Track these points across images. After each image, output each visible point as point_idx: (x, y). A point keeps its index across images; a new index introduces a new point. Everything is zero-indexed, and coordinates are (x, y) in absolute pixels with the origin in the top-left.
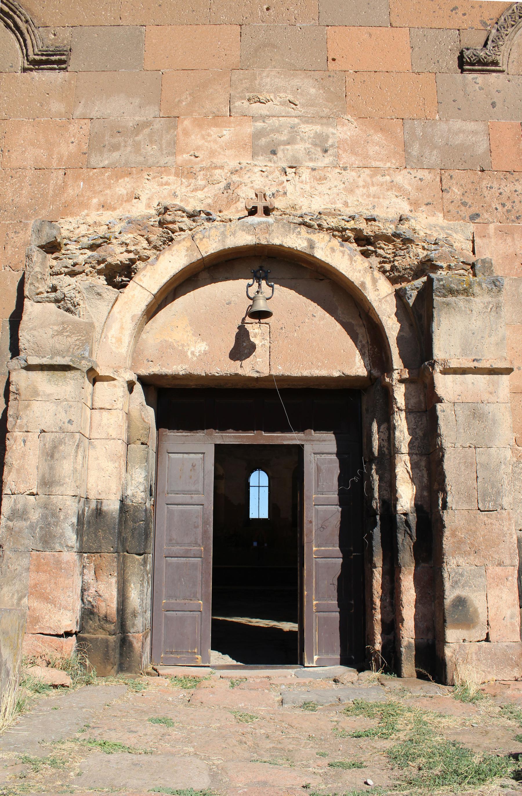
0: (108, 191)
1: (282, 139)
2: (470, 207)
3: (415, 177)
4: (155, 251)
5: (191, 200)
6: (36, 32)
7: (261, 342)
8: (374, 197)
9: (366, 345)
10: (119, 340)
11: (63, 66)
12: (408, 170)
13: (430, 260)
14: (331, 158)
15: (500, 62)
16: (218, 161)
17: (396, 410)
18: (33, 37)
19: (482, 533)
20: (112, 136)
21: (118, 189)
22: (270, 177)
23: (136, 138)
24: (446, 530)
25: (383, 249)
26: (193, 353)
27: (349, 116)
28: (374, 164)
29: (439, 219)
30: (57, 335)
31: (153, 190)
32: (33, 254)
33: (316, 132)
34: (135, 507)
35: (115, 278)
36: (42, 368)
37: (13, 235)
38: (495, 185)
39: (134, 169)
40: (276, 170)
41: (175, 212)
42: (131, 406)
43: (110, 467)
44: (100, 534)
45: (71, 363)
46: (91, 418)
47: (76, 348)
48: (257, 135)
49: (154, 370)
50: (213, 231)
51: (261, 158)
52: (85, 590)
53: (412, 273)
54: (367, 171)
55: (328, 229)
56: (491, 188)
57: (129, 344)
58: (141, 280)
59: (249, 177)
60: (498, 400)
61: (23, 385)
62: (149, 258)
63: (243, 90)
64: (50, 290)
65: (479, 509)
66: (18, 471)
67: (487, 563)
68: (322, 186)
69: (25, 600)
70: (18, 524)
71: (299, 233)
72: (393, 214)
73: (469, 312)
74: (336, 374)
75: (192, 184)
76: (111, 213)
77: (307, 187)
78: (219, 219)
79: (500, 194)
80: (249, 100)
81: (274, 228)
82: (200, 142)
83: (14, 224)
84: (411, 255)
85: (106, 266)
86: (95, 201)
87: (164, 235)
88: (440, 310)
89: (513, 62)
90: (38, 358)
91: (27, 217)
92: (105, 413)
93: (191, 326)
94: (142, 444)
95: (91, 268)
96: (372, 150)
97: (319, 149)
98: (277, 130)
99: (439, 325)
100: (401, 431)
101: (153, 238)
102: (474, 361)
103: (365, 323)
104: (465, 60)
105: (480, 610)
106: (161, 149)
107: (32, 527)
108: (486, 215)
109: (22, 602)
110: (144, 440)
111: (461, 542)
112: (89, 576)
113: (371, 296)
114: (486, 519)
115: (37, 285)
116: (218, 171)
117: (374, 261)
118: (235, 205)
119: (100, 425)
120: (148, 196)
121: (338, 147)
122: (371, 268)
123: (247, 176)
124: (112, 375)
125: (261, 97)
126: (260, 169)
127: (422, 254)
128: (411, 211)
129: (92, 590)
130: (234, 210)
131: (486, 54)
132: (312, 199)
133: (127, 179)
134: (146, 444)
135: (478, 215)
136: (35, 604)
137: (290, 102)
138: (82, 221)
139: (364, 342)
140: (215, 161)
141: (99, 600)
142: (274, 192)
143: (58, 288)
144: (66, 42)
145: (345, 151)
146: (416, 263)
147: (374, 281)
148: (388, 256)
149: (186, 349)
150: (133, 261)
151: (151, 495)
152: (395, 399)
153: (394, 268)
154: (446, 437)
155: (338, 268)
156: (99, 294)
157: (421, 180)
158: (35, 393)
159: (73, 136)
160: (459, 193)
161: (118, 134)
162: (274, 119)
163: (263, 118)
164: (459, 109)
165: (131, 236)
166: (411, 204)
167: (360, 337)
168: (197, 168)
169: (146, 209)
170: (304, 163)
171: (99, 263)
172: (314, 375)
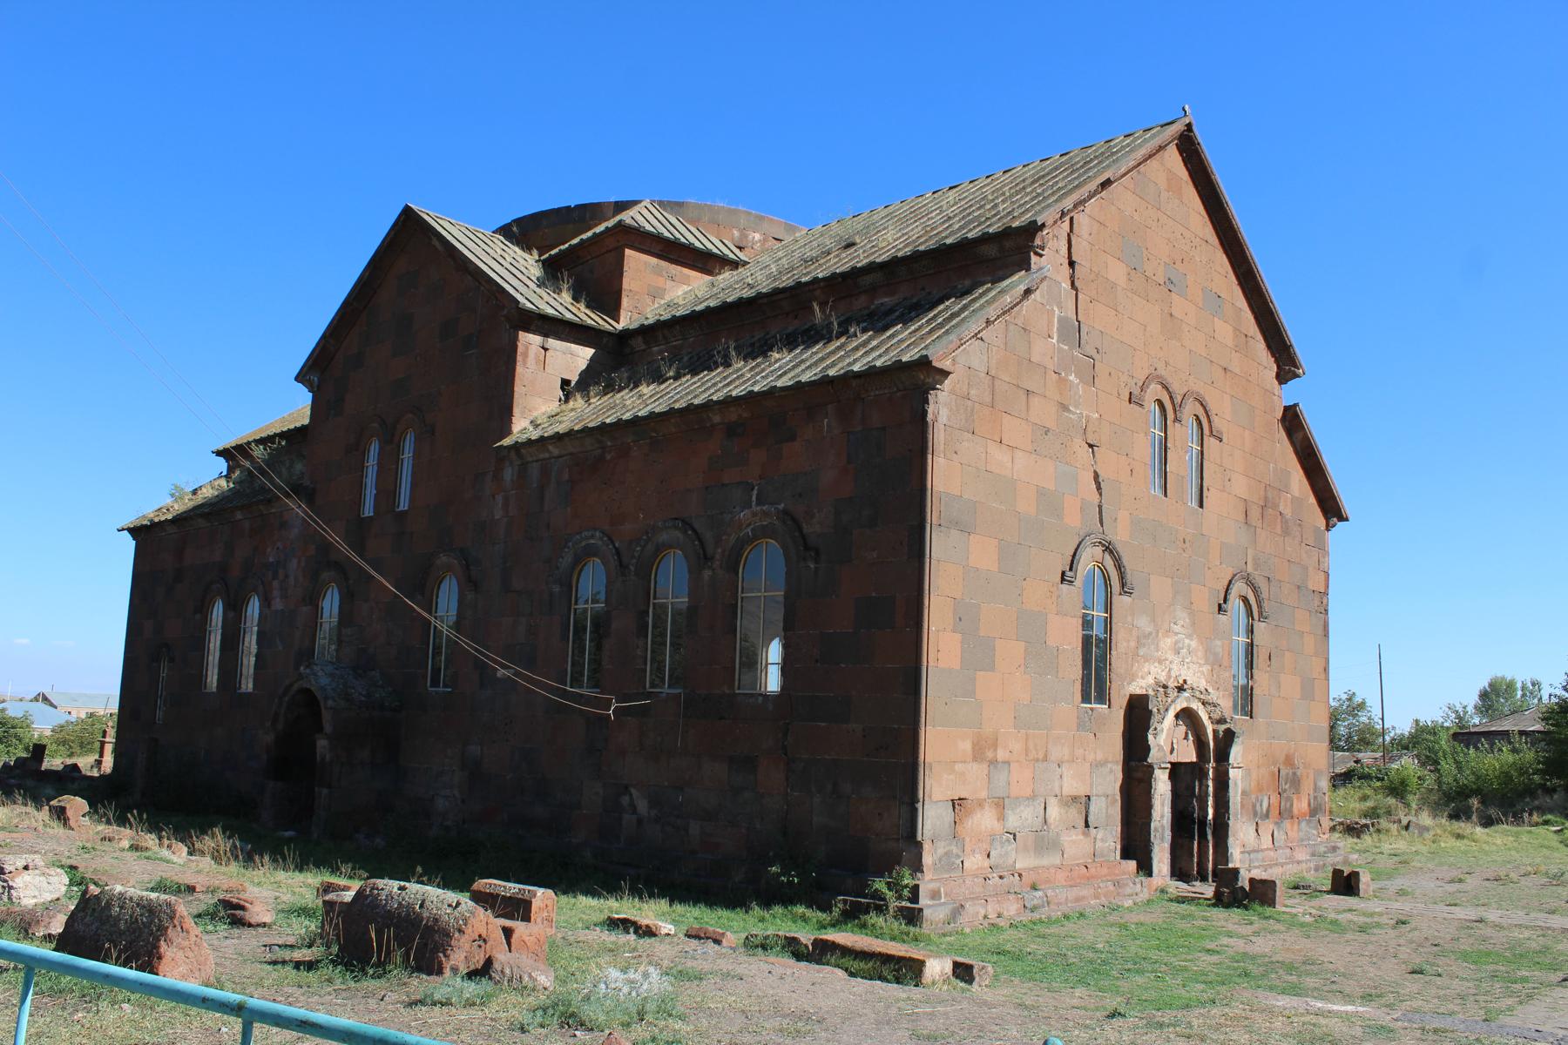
28: (1200, 661)
48: (1176, 643)
163: (1177, 634)
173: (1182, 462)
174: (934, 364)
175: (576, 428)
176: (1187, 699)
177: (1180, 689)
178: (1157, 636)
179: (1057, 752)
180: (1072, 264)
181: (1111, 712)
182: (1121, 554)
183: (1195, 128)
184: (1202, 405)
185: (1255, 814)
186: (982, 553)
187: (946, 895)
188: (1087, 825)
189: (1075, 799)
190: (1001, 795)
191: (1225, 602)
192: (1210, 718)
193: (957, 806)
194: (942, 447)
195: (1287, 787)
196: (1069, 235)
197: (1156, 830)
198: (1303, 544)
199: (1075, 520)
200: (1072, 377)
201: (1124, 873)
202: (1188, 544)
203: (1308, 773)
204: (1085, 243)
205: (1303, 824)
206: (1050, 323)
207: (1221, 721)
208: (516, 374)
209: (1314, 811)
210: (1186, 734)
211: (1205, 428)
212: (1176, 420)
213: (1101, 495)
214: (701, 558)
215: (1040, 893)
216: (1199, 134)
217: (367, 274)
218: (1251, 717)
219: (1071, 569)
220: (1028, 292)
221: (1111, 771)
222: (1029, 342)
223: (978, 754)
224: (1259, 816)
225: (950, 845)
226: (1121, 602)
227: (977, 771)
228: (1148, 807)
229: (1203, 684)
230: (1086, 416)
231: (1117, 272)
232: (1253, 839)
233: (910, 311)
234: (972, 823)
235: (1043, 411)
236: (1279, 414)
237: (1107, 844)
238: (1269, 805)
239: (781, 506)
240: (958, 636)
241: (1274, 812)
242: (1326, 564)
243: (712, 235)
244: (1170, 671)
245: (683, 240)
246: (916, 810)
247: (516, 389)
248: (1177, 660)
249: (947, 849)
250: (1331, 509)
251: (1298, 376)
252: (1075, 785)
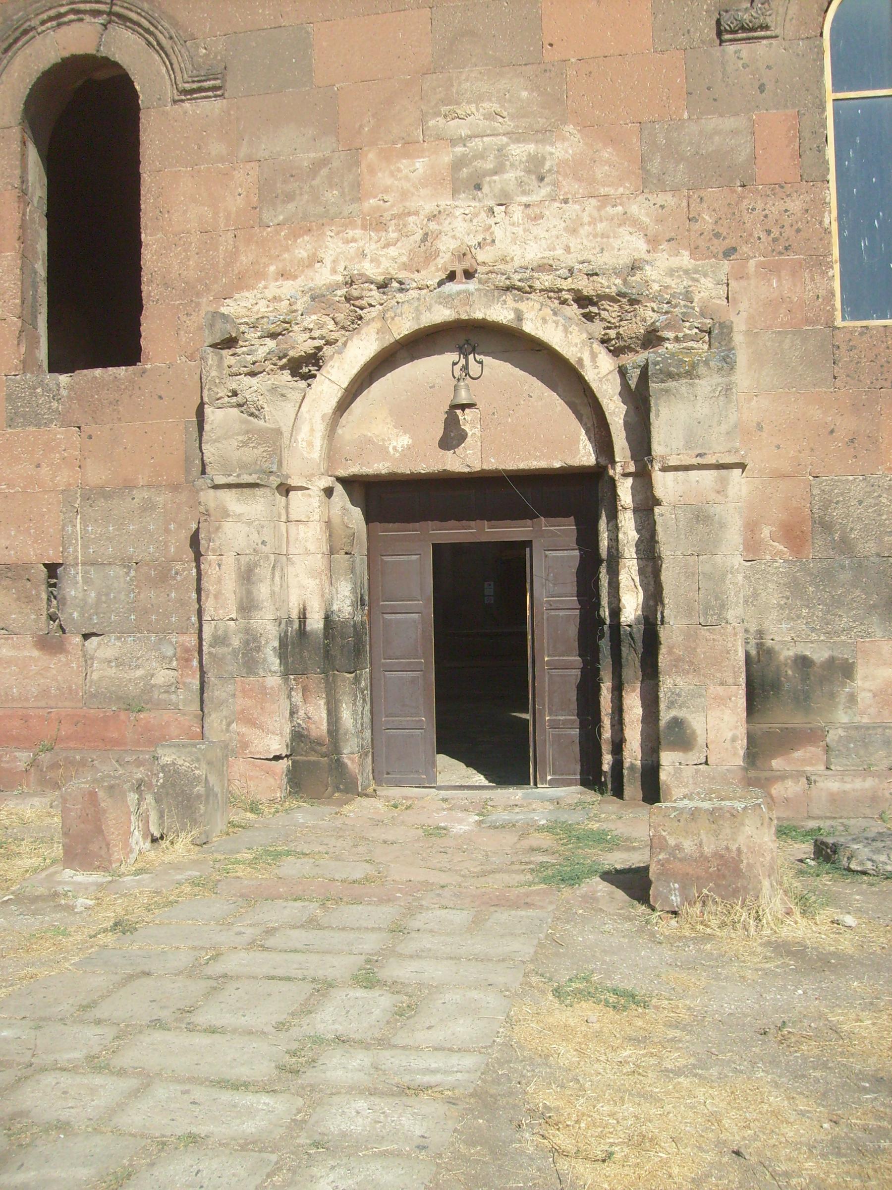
0: (286, 256)
1: (488, 168)
2: (724, 238)
3: (654, 204)
4: (343, 332)
5: (383, 259)
6: (183, 51)
7: (471, 430)
8: (603, 236)
9: (592, 428)
10: (310, 444)
11: (219, 93)
12: (646, 196)
13: (655, 331)
14: (549, 189)
15: (772, 25)
16: (412, 205)
17: (620, 508)
18: (180, 58)
19: (703, 650)
20: (284, 182)
21: (297, 251)
22: (475, 221)
23: (313, 183)
24: (662, 646)
25: (608, 311)
26: (395, 448)
27: (572, 126)
28: (603, 191)
29: (685, 260)
30: (242, 446)
31: (337, 249)
32: (207, 356)
33: (530, 154)
34: (342, 622)
35: (302, 368)
36: (229, 486)
37: (184, 318)
38: (760, 205)
39: (314, 224)
40: (482, 211)
41: (362, 285)
42: (332, 512)
43: (312, 584)
44: (306, 654)
45: (258, 481)
46: (287, 532)
47: (264, 460)
48: (458, 164)
49: (353, 470)
50: (406, 306)
51: (462, 196)
52: (294, 713)
53: (639, 342)
54: (593, 202)
55: (541, 290)
56: (753, 209)
57: (322, 447)
58: (329, 372)
59: (450, 224)
60: (726, 500)
61: (212, 505)
62: (338, 341)
63: (437, 103)
64: (230, 394)
65: (700, 624)
66: (216, 597)
67: (708, 682)
68: (538, 227)
69: (234, 725)
70: (220, 650)
71: (505, 301)
72: (624, 260)
73: (693, 398)
74: (557, 465)
75: (382, 239)
76: (292, 282)
77: (520, 231)
78: (414, 285)
79: (766, 216)
80: (445, 116)
81: (475, 298)
82: (389, 181)
83: (186, 303)
84: (638, 318)
85: (289, 360)
86: (272, 268)
87: (351, 314)
88: (657, 399)
89: (791, 20)
90: (224, 477)
91: (198, 295)
92: (301, 527)
93: (391, 417)
94: (346, 553)
95: (272, 366)
96: (600, 172)
97: (533, 177)
98: (482, 156)
99: (657, 416)
100: (625, 533)
101: (340, 317)
102: (697, 456)
103: (590, 401)
104: (722, 28)
105: (698, 732)
106: (342, 194)
107: (235, 653)
108: (745, 249)
109: (231, 728)
110: (347, 549)
111: (679, 659)
112: (297, 697)
113: (590, 375)
114: (708, 634)
115: (216, 390)
116: (411, 219)
117: (597, 328)
118: (434, 262)
119: (297, 539)
120: (332, 258)
121: (558, 172)
122: (590, 339)
123: (447, 222)
124: (305, 485)
125: (459, 112)
126: (462, 211)
128: (649, 252)
129: (301, 713)
130: (433, 269)
131: (752, 16)
132: (526, 246)
133: (306, 238)
134: (351, 554)
135: (734, 249)
136: (244, 729)
137: (496, 114)
138: (259, 296)
139: (589, 425)
140: (408, 204)
141: (308, 722)
142: (480, 240)
143: (239, 392)
144: (219, 58)
145: (566, 176)
146: (642, 331)
147: (594, 356)
148: (613, 321)
149: (386, 444)
150: (319, 349)
151: (363, 604)
152: (619, 496)
153: (619, 336)
154: (664, 544)
155: (550, 344)
156: (283, 395)
157: (662, 207)
158: (226, 514)
159: (241, 186)
160: (710, 221)
161: (292, 179)
162: (477, 140)
163: (463, 141)
164: (715, 100)
165: (314, 317)
166: (648, 242)
167: (584, 418)
168: (387, 215)
169: (331, 275)
170: (515, 198)
171: (280, 358)
172: (532, 468)
176: (447, 300)
207: (651, 339)
221: (148, 507)
237: (140, 673)
248: (464, 204)
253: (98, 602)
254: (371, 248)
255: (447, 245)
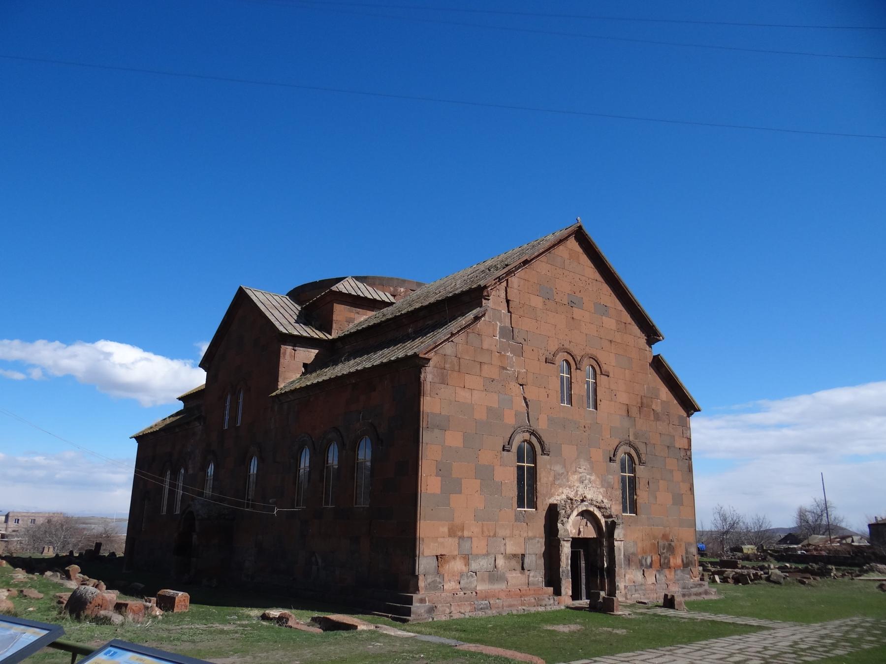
16: (575, 484)
48: (581, 477)
113: (602, 522)
127: (609, 513)
158: (564, 546)
163: (581, 473)
173: (579, 390)
174: (421, 356)
175: (298, 388)
176: (585, 505)
177: (582, 501)
178: (568, 474)
179: (501, 532)
180: (508, 301)
181: (537, 512)
182: (541, 435)
183: (584, 228)
184: (595, 360)
185: (642, 565)
186: (454, 439)
187: (429, 602)
188: (523, 569)
189: (515, 556)
190: (467, 553)
191: (614, 456)
192: (603, 515)
193: (439, 558)
194: (429, 392)
195: (664, 551)
196: (506, 288)
197: (563, 571)
198: (671, 425)
199: (510, 419)
200: (509, 354)
201: (545, 594)
202: (587, 428)
203: (680, 544)
204: (515, 291)
205: (679, 572)
206: (495, 330)
207: (610, 516)
208: (280, 362)
209: (686, 565)
210: (587, 523)
211: (598, 369)
212: (577, 368)
213: (528, 408)
214: (342, 447)
215: (486, 602)
216: (588, 230)
217: (226, 317)
218: (636, 515)
219: (508, 444)
220: (477, 318)
221: (538, 542)
222: (482, 340)
223: (452, 533)
224: (645, 566)
225: (435, 577)
226: (541, 459)
227: (454, 541)
228: (558, 560)
229: (600, 498)
230: (518, 371)
231: (537, 302)
232: (641, 577)
233: (421, 332)
234: (449, 567)
235: (490, 371)
236: (650, 360)
238: (652, 561)
239: (370, 421)
240: (440, 478)
241: (656, 565)
242: (688, 434)
243: (380, 290)
244: (577, 491)
245: (362, 295)
246: (415, 560)
247: (280, 369)
248: (581, 486)
249: (433, 579)
250: (690, 407)
251: (659, 340)
252: (514, 549)
253: (530, 563)
254: (570, 492)
255: (579, 493)
